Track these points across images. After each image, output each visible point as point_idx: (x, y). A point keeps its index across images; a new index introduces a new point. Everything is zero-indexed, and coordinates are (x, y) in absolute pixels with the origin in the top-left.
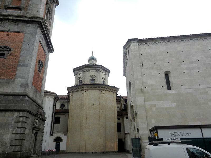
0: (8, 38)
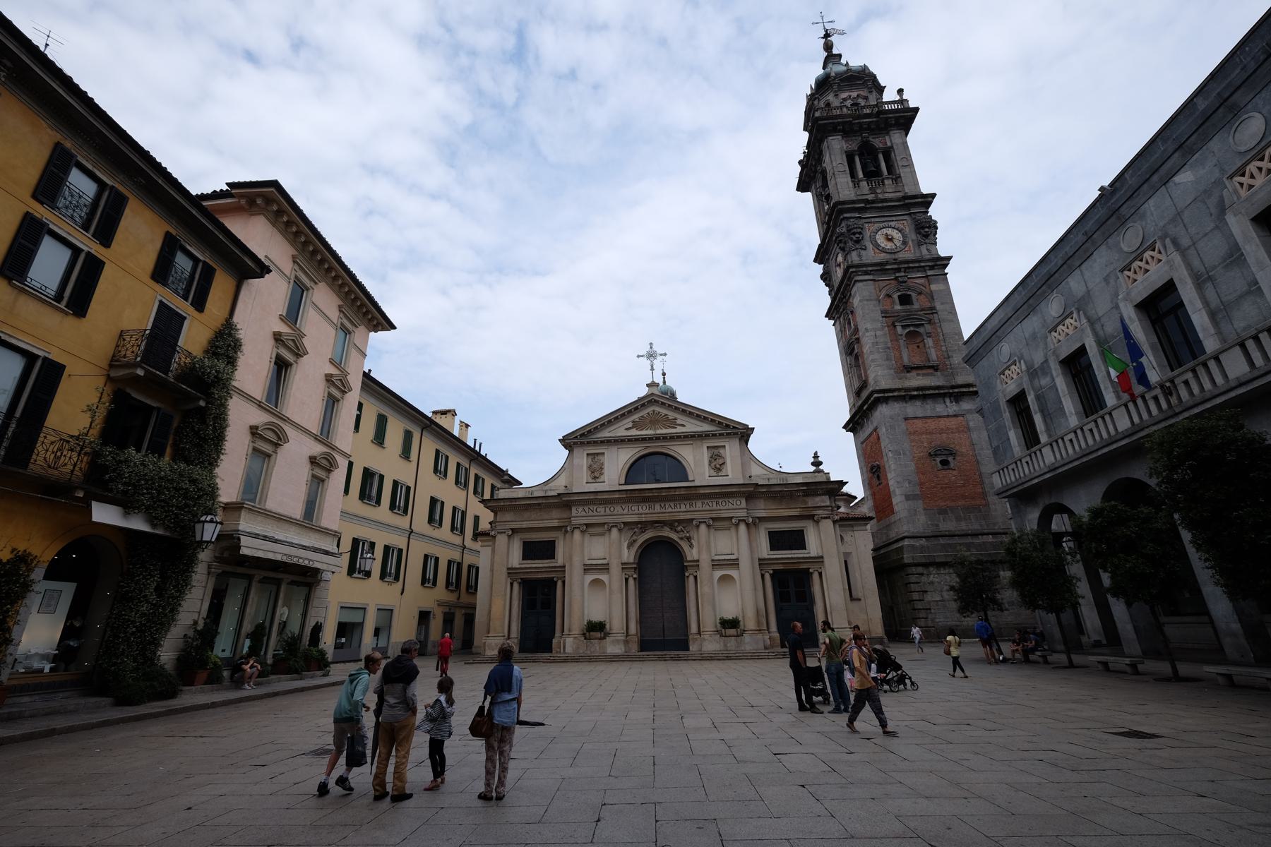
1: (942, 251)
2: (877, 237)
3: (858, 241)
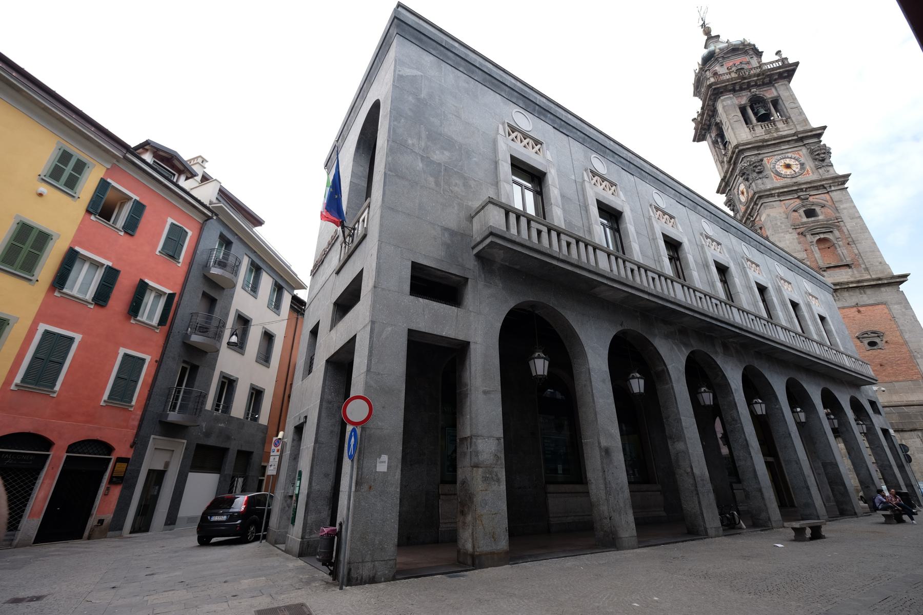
0: (864, 317)
1: (840, 170)
2: (777, 166)
3: (760, 172)
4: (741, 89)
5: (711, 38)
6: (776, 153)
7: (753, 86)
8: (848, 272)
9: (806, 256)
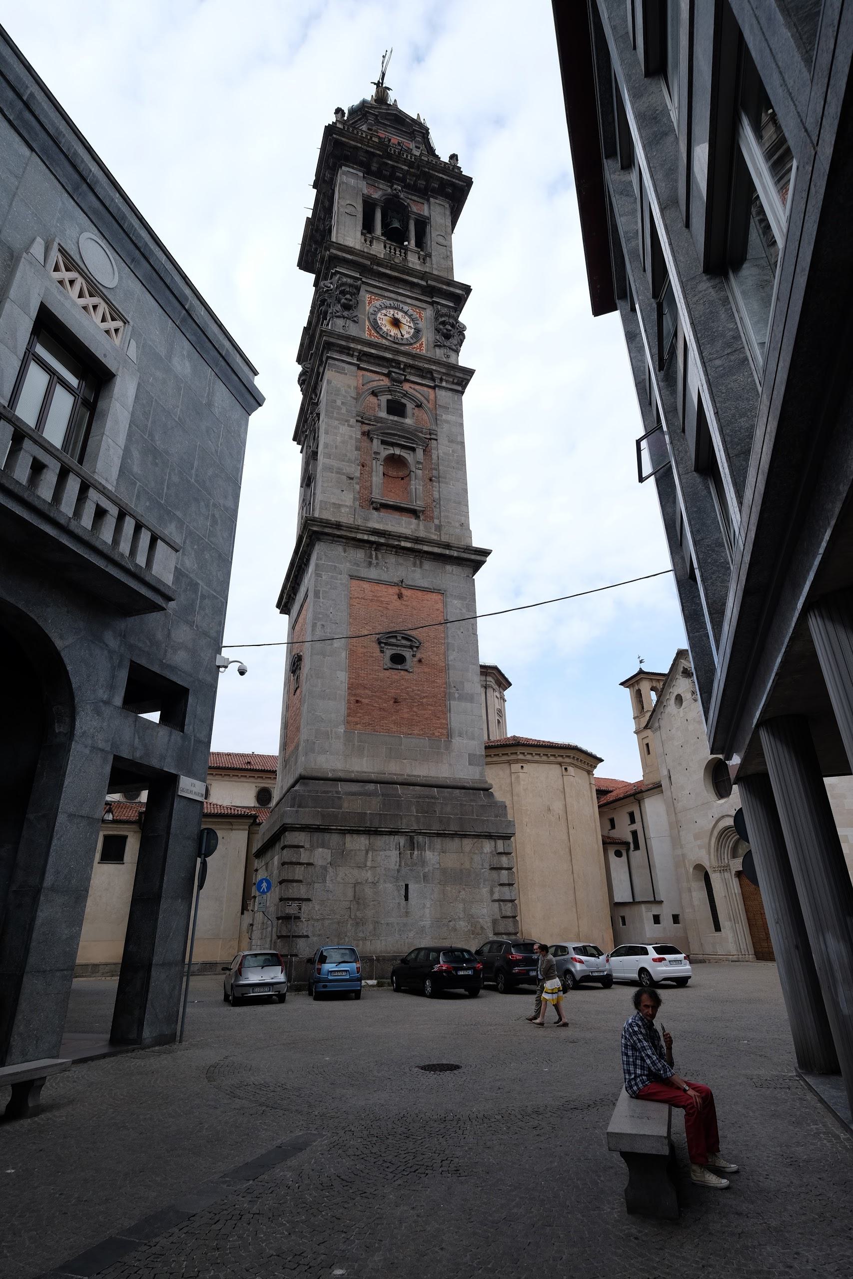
0: (403, 607)
1: (464, 359)
2: (379, 315)
3: (347, 307)
4: (379, 175)
5: (375, 84)
6: (387, 294)
7: (398, 179)
8: (410, 524)
9: (358, 474)
